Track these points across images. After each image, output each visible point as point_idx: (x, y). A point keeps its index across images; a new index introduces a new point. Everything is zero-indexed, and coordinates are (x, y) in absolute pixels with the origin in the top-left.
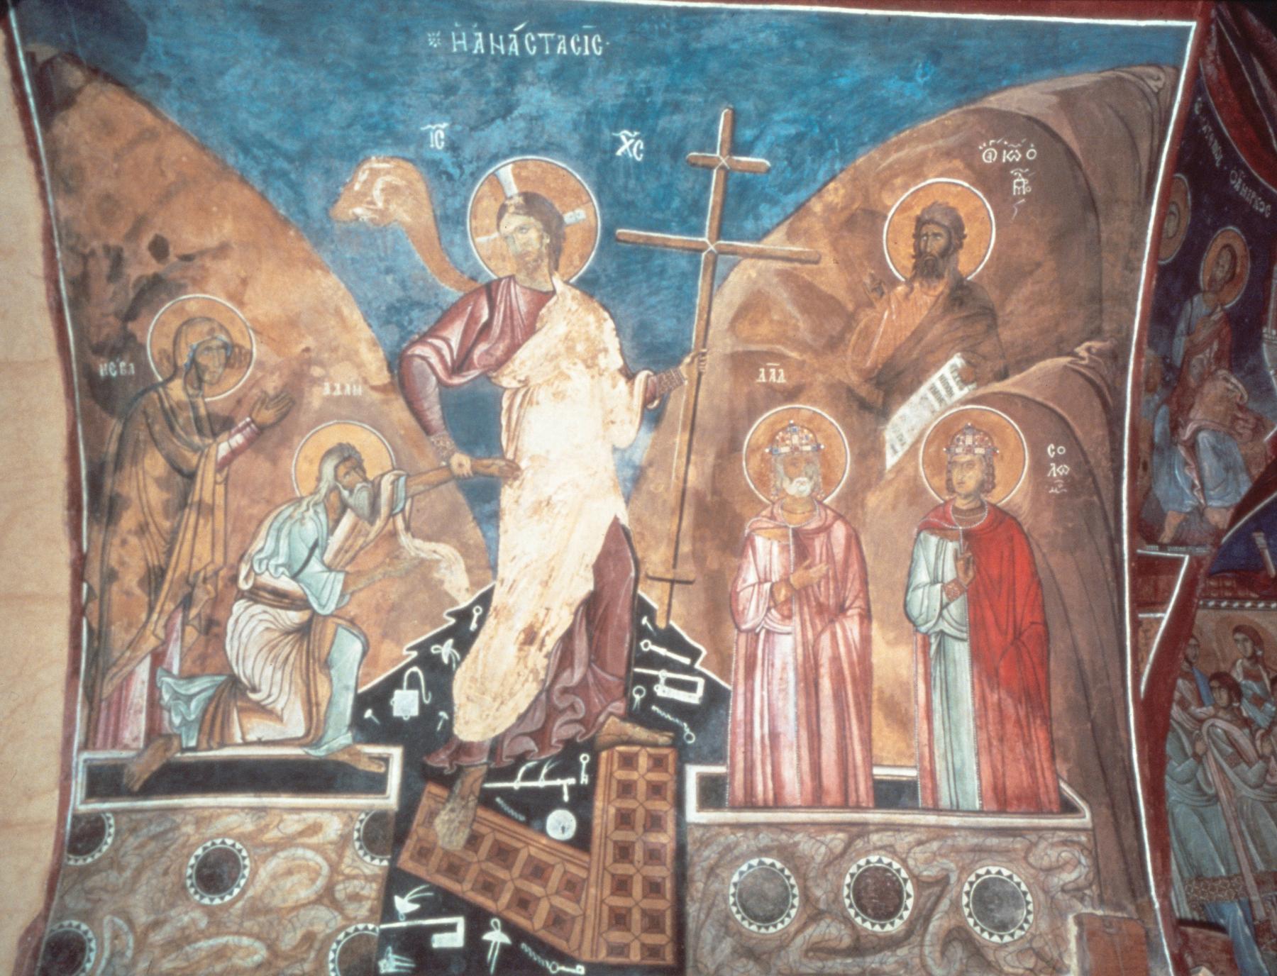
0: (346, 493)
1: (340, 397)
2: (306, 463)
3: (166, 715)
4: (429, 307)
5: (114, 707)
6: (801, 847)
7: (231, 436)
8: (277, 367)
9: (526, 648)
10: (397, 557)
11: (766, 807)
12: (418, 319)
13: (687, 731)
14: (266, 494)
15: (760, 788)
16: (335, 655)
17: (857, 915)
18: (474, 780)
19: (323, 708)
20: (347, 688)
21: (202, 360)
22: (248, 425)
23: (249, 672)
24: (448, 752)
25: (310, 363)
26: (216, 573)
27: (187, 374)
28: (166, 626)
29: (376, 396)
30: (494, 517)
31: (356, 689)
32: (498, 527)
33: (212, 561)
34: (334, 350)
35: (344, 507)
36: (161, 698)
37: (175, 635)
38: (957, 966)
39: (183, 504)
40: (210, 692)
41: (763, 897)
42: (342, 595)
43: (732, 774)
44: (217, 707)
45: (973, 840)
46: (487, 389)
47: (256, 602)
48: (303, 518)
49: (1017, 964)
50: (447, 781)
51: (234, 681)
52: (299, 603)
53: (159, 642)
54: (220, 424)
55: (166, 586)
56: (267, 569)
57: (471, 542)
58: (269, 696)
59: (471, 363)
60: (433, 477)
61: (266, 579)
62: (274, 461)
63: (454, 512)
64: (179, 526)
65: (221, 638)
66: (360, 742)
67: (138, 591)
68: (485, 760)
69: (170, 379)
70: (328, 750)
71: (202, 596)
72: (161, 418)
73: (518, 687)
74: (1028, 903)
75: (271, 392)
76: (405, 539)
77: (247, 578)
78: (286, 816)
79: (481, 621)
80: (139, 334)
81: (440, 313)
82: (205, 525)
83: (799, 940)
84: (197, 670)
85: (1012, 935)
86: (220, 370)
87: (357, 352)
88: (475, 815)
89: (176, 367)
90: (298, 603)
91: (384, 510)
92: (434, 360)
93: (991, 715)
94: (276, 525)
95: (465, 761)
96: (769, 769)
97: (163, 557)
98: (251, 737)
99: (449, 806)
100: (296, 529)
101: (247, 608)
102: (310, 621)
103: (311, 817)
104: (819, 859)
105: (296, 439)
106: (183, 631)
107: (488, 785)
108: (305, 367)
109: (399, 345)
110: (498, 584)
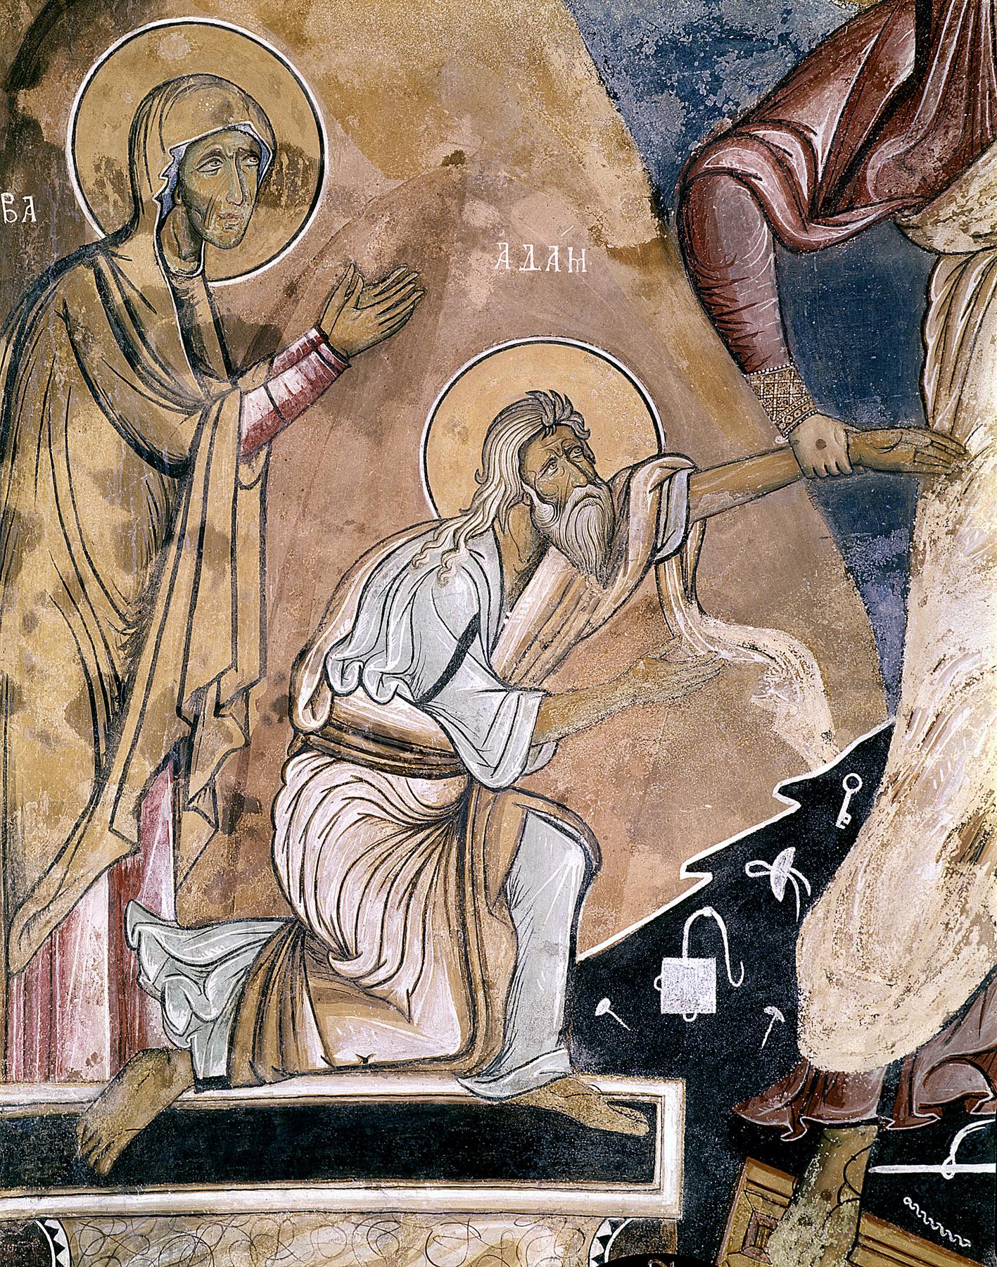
0: (545, 511)
1: (533, 277)
2: (456, 440)
3: (154, 1006)
4: (764, 45)
5: (39, 992)
7: (273, 375)
8: (384, 204)
9: (964, 868)
10: (663, 659)
12: (737, 74)
14: (356, 512)
16: (523, 875)
18: (850, 1153)
19: (499, 994)
20: (551, 949)
21: (201, 185)
22: (313, 345)
23: (329, 912)
24: (789, 1096)
25: (462, 193)
26: (245, 692)
27: (162, 223)
28: (137, 813)
29: (626, 275)
30: (900, 568)
31: (573, 953)
32: (905, 591)
33: (234, 665)
34: (523, 158)
35: (543, 544)
36: (140, 971)
37: (159, 833)
39: (166, 537)
40: (247, 958)
42: (535, 745)
44: (264, 992)
46: (891, 256)
47: (340, 759)
48: (445, 567)
50: (793, 1156)
51: (299, 933)
52: (441, 762)
53: (127, 848)
54: (244, 348)
55: (131, 721)
56: (361, 683)
57: (840, 626)
58: (378, 966)
59: (860, 192)
60: (757, 472)
61: (358, 706)
62: (377, 434)
63: (803, 557)
64: (154, 586)
65: (265, 837)
66: (587, 1069)
67: (68, 733)
68: (873, 1114)
69: (123, 235)
70: (515, 1083)
71: (215, 743)
72: (104, 330)
73: (946, 954)
75: (370, 267)
76: (682, 617)
77: (311, 701)
78: (438, 1230)
79: (861, 809)
80: (44, 120)
81: (790, 58)
82: (215, 584)
84: (214, 910)
86: (246, 211)
87: (578, 164)
88: (858, 1234)
89: (136, 200)
90: (434, 759)
91: (637, 551)
92: (769, 184)
94: (381, 583)
95: (827, 1114)
97: (119, 656)
98: (345, 1056)
99: (797, 1212)
100: (424, 594)
101: (317, 771)
102: (464, 799)
103: (492, 1229)
105: (429, 382)
106: (177, 822)
107: (879, 1169)
108: (452, 203)
109: (682, 147)
110: (900, 723)
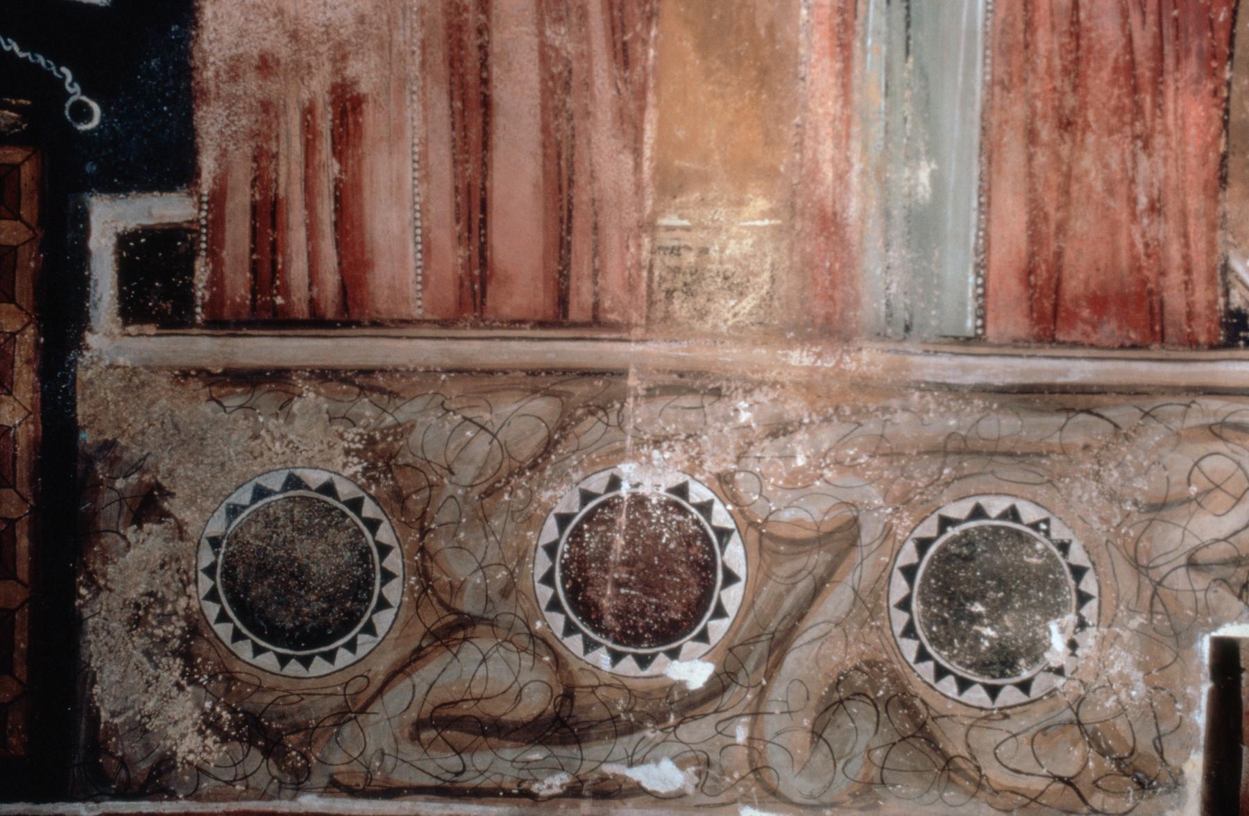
6: (416, 438)
11: (316, 322)
13: (75, 92)
15: (298, 269)
17: (570, 629)
38: (856, 768)
41: (296, 576)
43: (217, 223)
45: (947, 421)
49: (1029, 764)
74: (1083, 598)
83: (397, 698)
85: (1025, 686)
93: (1046, 42)
96: (326, 211)
104: (466, 473)
